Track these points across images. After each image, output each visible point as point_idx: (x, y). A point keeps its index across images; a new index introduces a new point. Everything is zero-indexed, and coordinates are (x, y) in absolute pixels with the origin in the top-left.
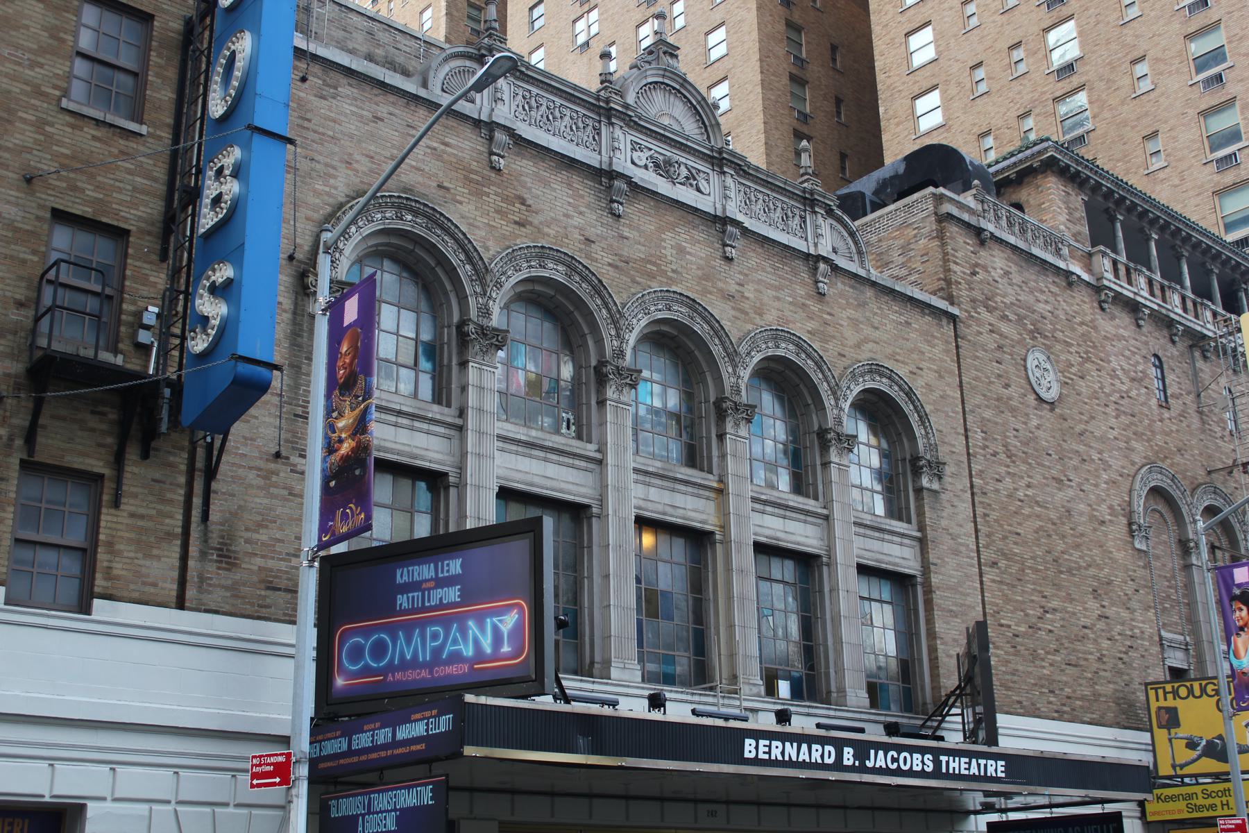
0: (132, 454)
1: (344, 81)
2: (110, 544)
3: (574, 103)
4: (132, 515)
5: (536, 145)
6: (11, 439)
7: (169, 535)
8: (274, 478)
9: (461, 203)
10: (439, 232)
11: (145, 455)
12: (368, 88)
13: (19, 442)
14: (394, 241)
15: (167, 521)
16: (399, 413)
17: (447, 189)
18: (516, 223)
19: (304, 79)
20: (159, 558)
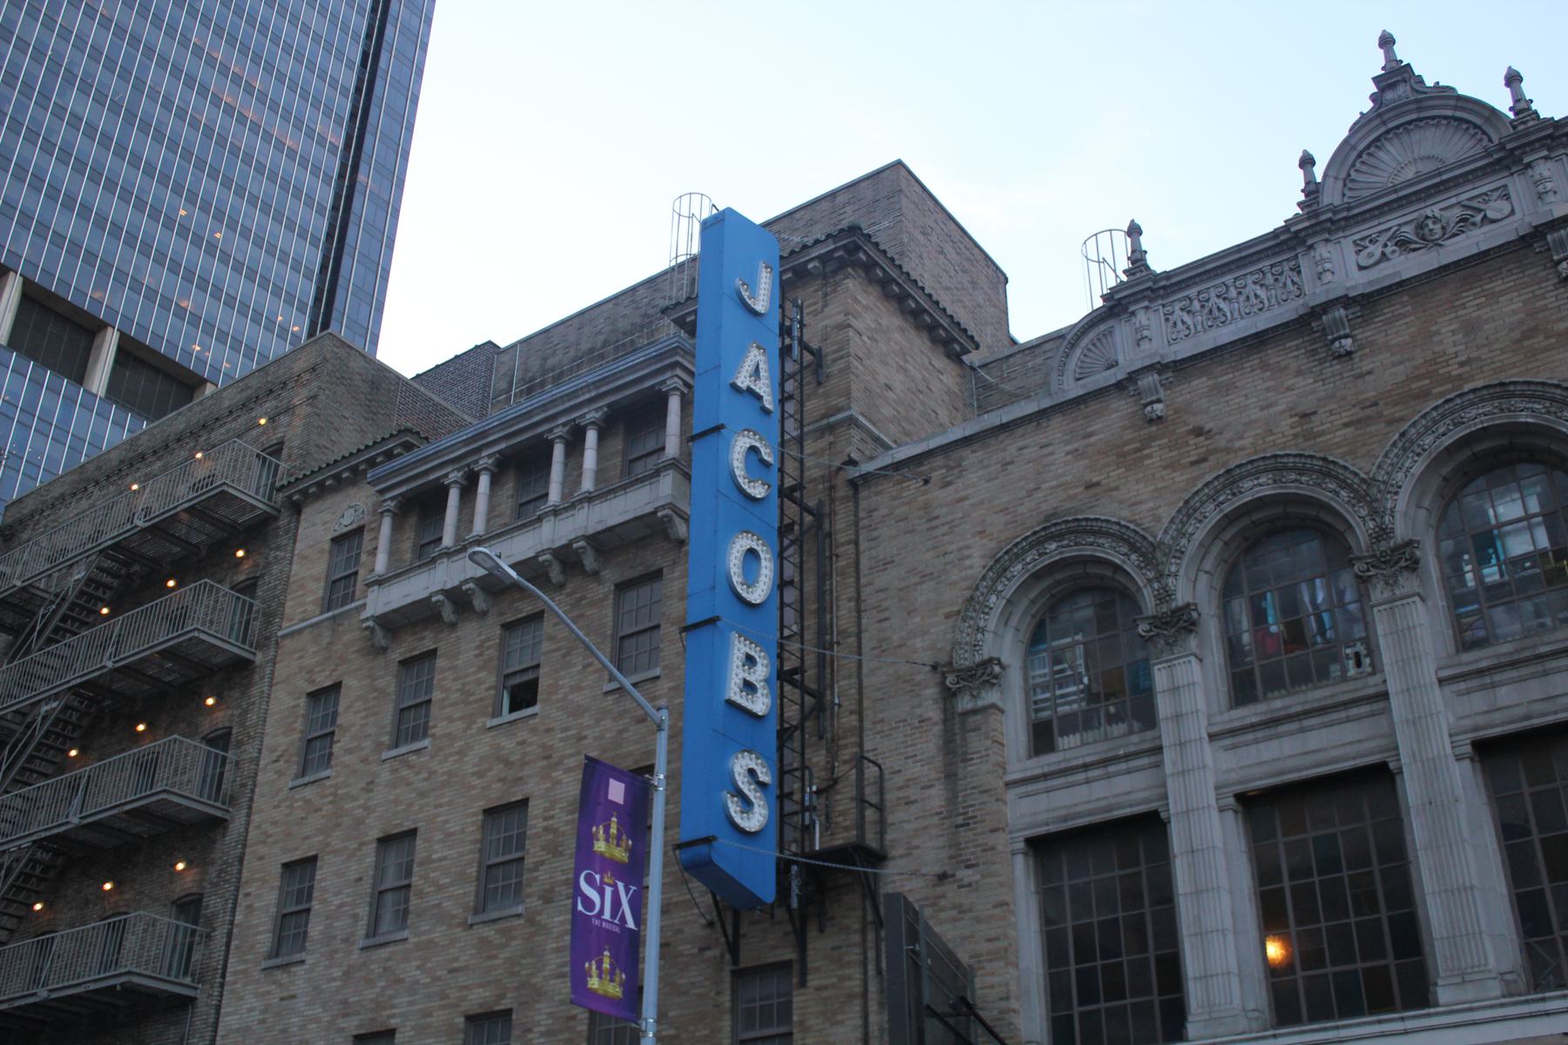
0: (812, 933)
1: (966, 452)
2: (802, 1023)
3: (1252, 263)
4: (818, 989)
5: (1202, 356)
6: (722, 956)
7: (851, 997)
8: (942, 902)
9: (1117, 489)
10: (1091, 539)
11: (822, 931)
12: (993, 441)
13: (728, 957)
14: (1059, 576)
15: (847, 984)
16: (1086, 767)
17: (1098, 484)
18: (1193, 463)
19: (926, 482)
20: (842, 1022)
